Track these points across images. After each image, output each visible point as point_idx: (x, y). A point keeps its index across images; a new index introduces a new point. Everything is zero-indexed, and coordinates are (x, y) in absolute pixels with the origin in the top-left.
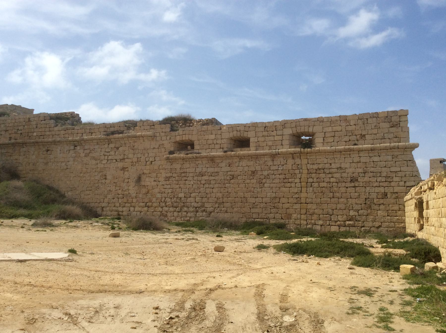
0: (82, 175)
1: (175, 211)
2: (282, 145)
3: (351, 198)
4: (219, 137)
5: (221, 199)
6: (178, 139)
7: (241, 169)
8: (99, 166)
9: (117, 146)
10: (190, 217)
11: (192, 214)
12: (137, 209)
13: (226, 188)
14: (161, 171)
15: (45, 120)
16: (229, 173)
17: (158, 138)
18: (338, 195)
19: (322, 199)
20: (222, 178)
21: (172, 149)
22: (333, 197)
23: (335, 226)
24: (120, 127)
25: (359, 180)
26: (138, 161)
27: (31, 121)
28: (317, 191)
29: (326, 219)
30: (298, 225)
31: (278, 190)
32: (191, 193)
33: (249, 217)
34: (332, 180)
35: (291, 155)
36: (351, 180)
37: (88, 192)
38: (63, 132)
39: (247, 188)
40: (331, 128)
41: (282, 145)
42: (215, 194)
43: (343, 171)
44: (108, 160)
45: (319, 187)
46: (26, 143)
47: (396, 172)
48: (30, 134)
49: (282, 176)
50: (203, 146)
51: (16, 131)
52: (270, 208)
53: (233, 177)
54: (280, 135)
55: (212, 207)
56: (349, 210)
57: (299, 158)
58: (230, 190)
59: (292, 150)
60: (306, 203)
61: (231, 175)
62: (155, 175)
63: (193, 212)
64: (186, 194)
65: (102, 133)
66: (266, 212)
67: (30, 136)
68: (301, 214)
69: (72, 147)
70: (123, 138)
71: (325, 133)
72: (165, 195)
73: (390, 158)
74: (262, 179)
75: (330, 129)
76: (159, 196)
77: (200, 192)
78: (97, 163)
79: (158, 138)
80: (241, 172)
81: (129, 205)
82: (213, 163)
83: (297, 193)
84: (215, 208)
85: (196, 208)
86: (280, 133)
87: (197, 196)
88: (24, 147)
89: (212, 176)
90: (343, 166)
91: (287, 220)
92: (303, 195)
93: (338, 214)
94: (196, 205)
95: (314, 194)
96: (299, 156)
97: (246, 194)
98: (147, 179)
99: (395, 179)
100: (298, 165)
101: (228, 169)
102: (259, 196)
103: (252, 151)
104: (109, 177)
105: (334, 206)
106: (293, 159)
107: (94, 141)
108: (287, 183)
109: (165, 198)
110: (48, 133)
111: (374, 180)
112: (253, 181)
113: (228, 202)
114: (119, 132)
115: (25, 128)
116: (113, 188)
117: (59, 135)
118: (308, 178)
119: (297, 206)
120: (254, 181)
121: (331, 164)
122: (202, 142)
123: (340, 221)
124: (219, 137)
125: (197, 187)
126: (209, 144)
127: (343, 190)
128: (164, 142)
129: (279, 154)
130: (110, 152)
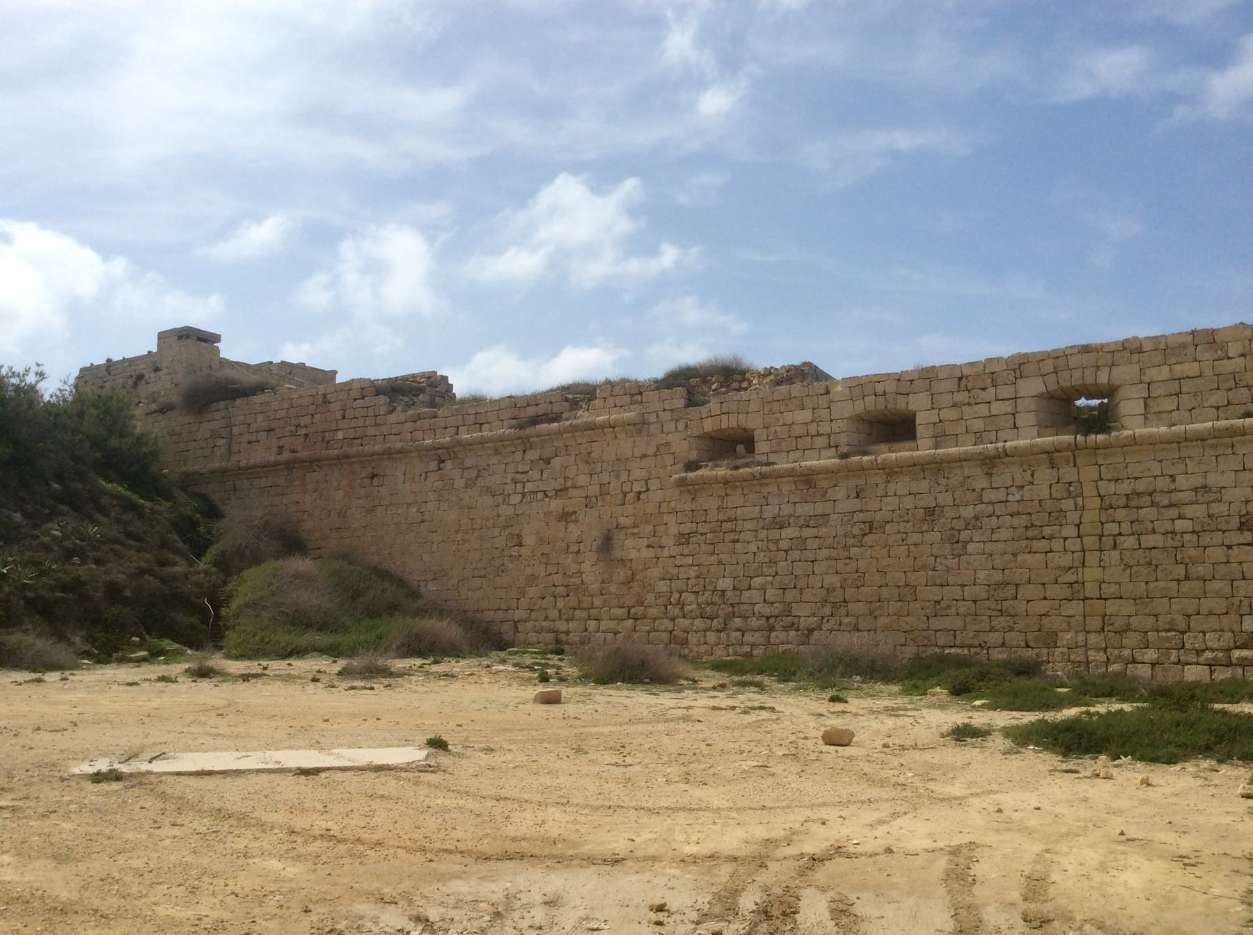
2: (1015, 427)
3: (1244, 578)
4: (824, 414)
5: (839, 592)
6: (708, 426)
7: (891, 502)
9: (546, 455)
10: (753, 645)
12: (605, 624)
13: (850, 558)
14: (666, 518)
16: (859, 517)
17: (652, 427)
18: (1200, 569)
19: (1151, 586)
20: (840, 531)
21: (693, 455)
22: (1187, 578)
23: (1197, 664)
24: (551, 402)
27: (330, 403)
28: (1132, 562)
29: (1168, 645)
30: (1079, 666)
31: (1011, 561)
32: (751, 578)
33: (926, 642)
34: (1180, 525)
35: (1044, 456)
36: (1242, 524)
38: (408, 426)
39: (915, 558)
40: (1166, 368)
41: (1015, 427)
42: (819, 578)
44: (524, 494)
45: (1140, 548)
46: (318, 460)
48: (328, 436)
49: (1022, 521)
50: (779, 444)
51: (293, 428)
52: (990, 617)
53: (871, 527)
54: (1008, 399)
55: (814, 615)
56: (1242, 616)
57: (1072, 464)
58: (863, 565)
59: (1048, 440)
60: (1101, 598)
61: (864, 522)
62: (649, 528)
63: (760, 630)
64: (738, 579)
65: (506, 424)
66: (976, 627)
67: (328, 442)
68: (1088, 632)
69: (433, 465)
70: (560, 433)
71: (1149, 384)
72: (679, 584)
74: (960, 531)
75: (1164, 373)
76: (662, 586)
77: (777, 573)
78: (496, 504)
80: (893, 511)
81: (584, 614)
82: (811, 491)
83: (1070, 568)
84: (823, 618)
85: (768, 618)
86: (1005, 392)
87: (769, 586)
88: (314, 471)
89: (808, 526)
90: (1212, 480)
91: (1045, 651)
92: (1091, 574)
93: (1205, 627)
94: (767, 610)
95: (1124, 570)
96: (1072, 458)
97: (912, 578)
98: (629, 542)
100: (1070, 484)
101: (854, 504)
102: (951, 580)
103: (923, 450)
104: (529, 540)
105: (1191, 606)
106: (1053, 467)
107: (486, 445)
108: (1036, 539)
109: (681, 593)
110: (372, 431)
112: (929, 537)
113: (858, 601)
114: (550, 416)
115: (314, 421)
116: (540, 570)
117: (399, 434)
118: (1103, 524)
119: (1074, 608)
120: (937, 536)
121: (1173, 478)
122: (776, 431)
123: (1213, 650)
124: (824, 414)
125: (767, 560)
126: (797, 437)
127: (1217, 554)
129: (1007, 455)
130: (528, 472)
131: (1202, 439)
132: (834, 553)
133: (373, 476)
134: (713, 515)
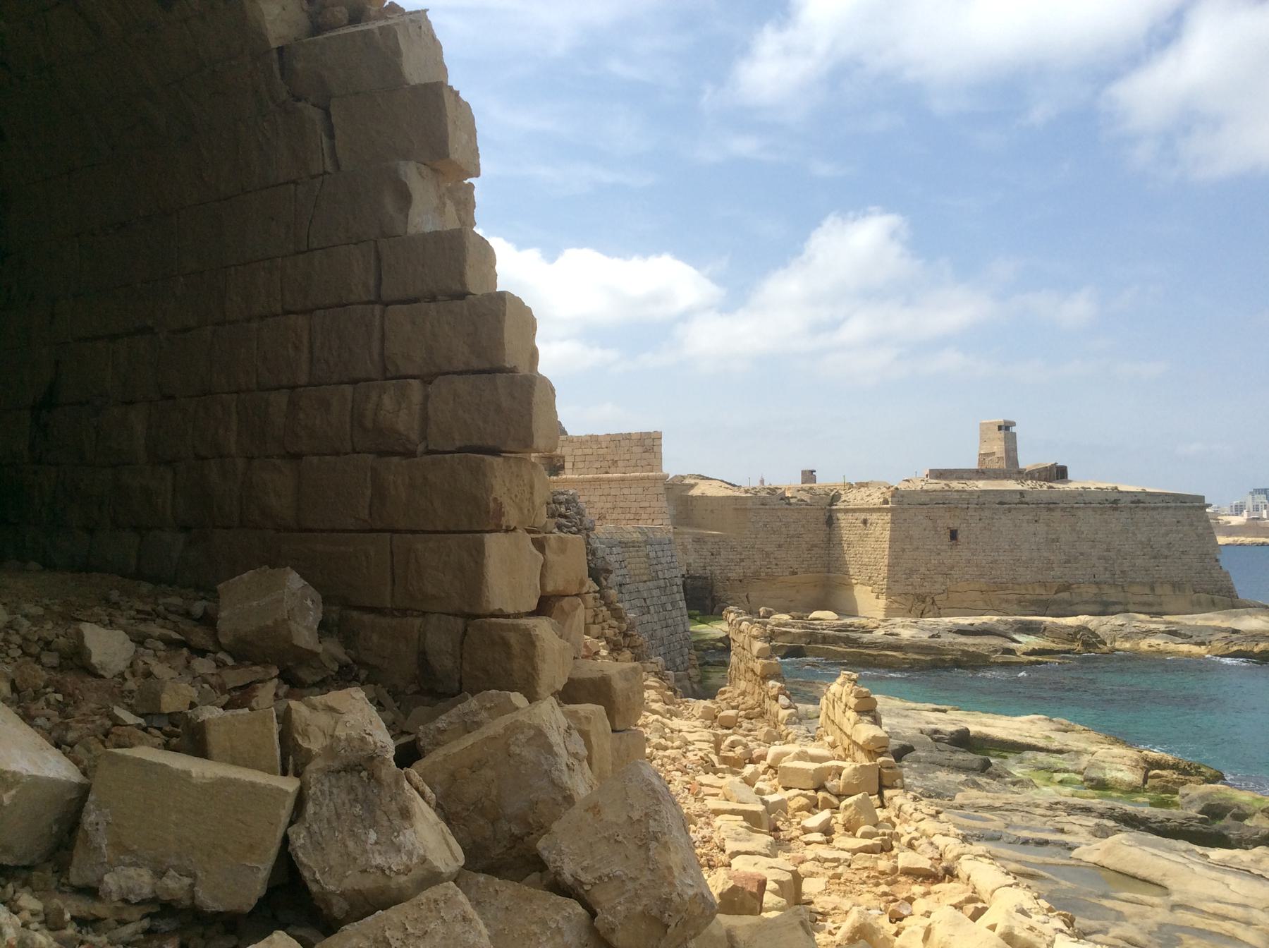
25: (607, 517)
43: (591, 505)
47: (645, 508)
73: (640, 490)
75: (579, 452)
90: (592, 499)
99: (644, 516)
111: (622, 517)
131: (589, 481)
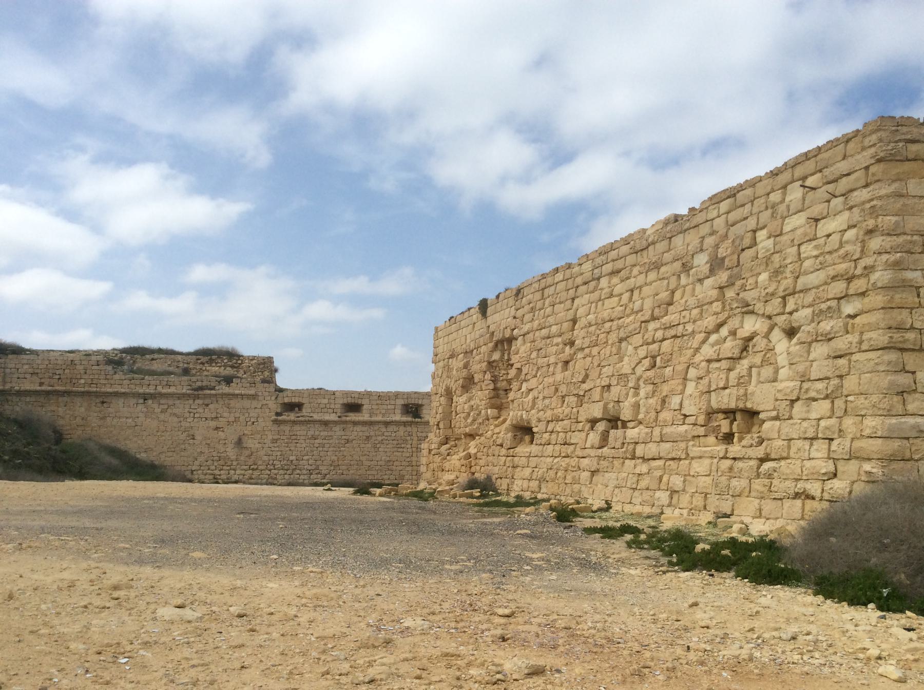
0: (159, 434)
1: (286, 474)
4: (332, 401)
6: (286, 400)
8: (183, 424)
10: (304, 480)
11: (306, 477)
12: (238, 472)
15: (98, 365)
16: (343, 437)
17: (260, 398)
20: (337, 442)
21: (279, 410)
26: (236, 420)
37: (170, 454)
44: (194, 418)
51: (51, 375)
53: (348, 441)
58: (345, 453)
59: (405, 419)
69: (141, 401)
72: (274, 458)
76: (266, 458)
79: (260, 398)
81: (228, 468)
86: (393, 402)
94: (310, 468)
97: (361, 458)
98: (250, 441)
101: (343, 433)
103: (364, 416)
104: (198, 437)
109: (274, 461)
119: (409, 468)
124: (332, 401)
128: (268, 402)
132: (335, 449)
133: (103, 402)
134: (287, 433)
